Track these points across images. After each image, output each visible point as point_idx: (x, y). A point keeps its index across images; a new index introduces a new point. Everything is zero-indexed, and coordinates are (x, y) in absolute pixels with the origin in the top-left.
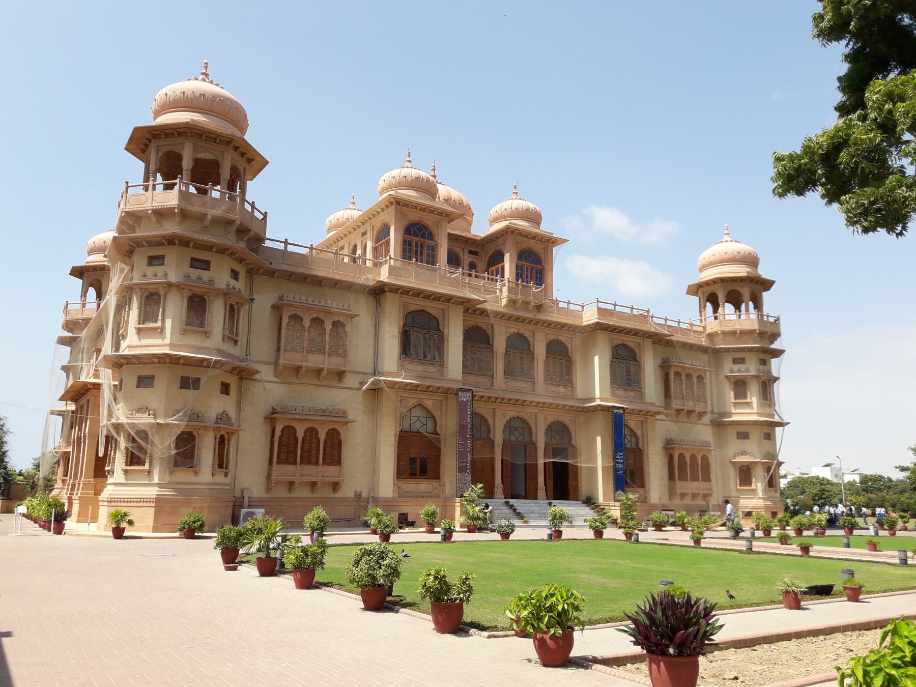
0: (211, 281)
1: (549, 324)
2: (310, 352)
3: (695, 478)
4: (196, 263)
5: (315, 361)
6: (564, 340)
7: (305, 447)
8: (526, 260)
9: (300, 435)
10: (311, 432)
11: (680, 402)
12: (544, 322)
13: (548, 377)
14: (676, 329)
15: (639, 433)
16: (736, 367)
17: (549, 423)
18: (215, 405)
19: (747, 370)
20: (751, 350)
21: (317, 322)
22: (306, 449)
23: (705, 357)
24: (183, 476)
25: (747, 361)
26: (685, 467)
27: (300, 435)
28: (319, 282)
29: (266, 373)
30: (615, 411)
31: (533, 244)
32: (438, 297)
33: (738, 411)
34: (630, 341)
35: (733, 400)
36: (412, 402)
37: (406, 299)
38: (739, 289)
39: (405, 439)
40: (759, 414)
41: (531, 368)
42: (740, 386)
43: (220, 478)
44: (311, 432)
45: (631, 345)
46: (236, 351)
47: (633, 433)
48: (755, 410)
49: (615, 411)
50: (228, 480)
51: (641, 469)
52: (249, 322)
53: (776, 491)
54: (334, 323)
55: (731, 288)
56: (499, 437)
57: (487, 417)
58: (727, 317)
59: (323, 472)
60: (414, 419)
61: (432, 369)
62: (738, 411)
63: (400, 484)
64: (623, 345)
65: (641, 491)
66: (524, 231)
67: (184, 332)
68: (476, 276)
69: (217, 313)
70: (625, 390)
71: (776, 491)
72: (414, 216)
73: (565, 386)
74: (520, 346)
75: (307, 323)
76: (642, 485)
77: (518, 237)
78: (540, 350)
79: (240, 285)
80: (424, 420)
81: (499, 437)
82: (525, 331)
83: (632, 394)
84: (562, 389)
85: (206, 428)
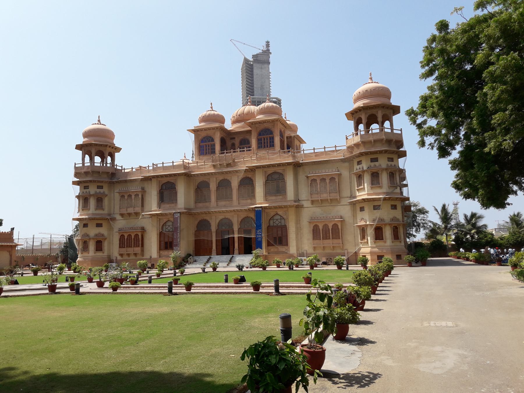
0: (89, 192)
1: (237, 171)
2: (129, 207)
3: (326, 237)
4: (86, 187)
5: (131, 210)
6: (250, 176)
7: (133, 241)
8: (263, 135)
9: (126, 238)
10: (130, 236)
11: (316, 195)
12: (236, 171)
13: (240, 196)
14: (317, 154)
15: (285, 217)
16: (358, 167)
17: (242, 218)
18: (93, 231)
19: (363, 168)
20: (361, 154)
21: (130, 196)
22: (128, 242)
23: (347, 164)
24: (85, 254)
25: (363, 162)
26: (327, 232)
27: (126, 238)
28: (126, 181)
29: (118, 217)
30: (256, 209)
31: (266, 125)
32: (170, 175)
33: (360, 194)
34: (279, 170)
35: (356, 188)
36: (165, 220)
37: (159, 179)
38: (361, 116)
39: (161, 235)
40: (368, 194)
41: (231, 194)
42: (360, 177)
43: (99, 254)
44: (130, 236)
45: (279, 171)
46: (106, 212)
47: (282, 218)
48: (366, 192)
49: (256, 209)
50: (106, 254)
51: (287, 236)
52: (114, 200)
53: (400, 242)
54: (135, 195)
55: (358, 117)
56: (214, 228)
57: (209, 220)
58: (386, 130)
59: (138, 250)
60: (167, 227)
61: (173, 205)
62: (360, 194)
63: (161, 252)
64: (275, 173)
65: (286, 247)
66: (262, 121)
67: (83, 210)
68: (227, 153)
69: (92, 202)
70: (276, 196)
71: (400, 242)
72: (203, 134)
73: (251, 199)
74: (224, 185)
75: (126, 197)
76: (287, 244)
77: (257, 125)
78: (235, 183)
79: (105, 190)
80: (171, 226)
81: (214, 228)
82: (228, 177)
83: (281, 197)
84: (249, 201)
85: (90, 239)
